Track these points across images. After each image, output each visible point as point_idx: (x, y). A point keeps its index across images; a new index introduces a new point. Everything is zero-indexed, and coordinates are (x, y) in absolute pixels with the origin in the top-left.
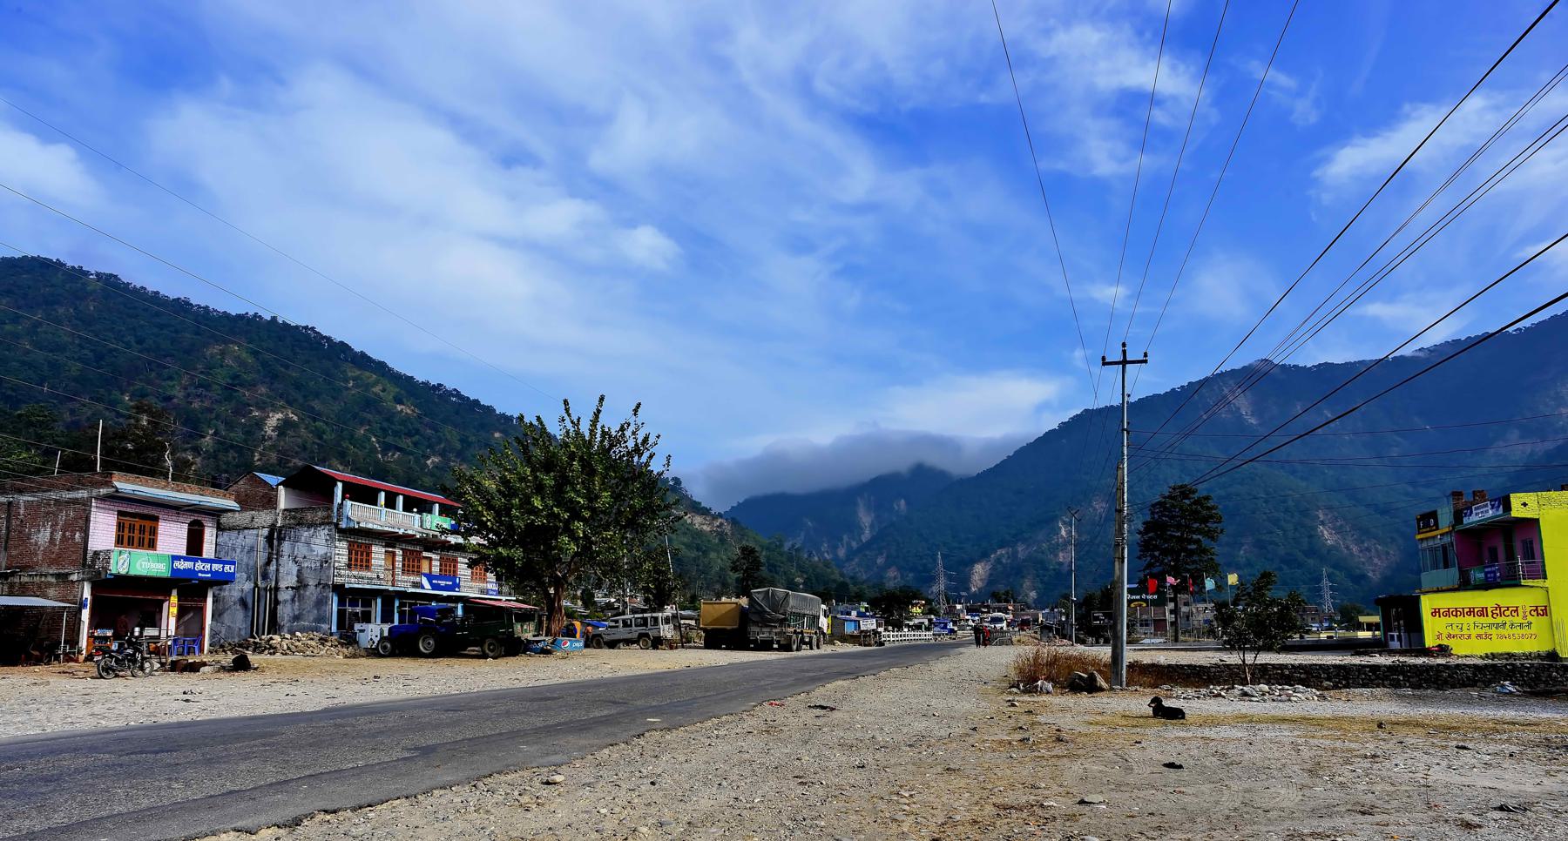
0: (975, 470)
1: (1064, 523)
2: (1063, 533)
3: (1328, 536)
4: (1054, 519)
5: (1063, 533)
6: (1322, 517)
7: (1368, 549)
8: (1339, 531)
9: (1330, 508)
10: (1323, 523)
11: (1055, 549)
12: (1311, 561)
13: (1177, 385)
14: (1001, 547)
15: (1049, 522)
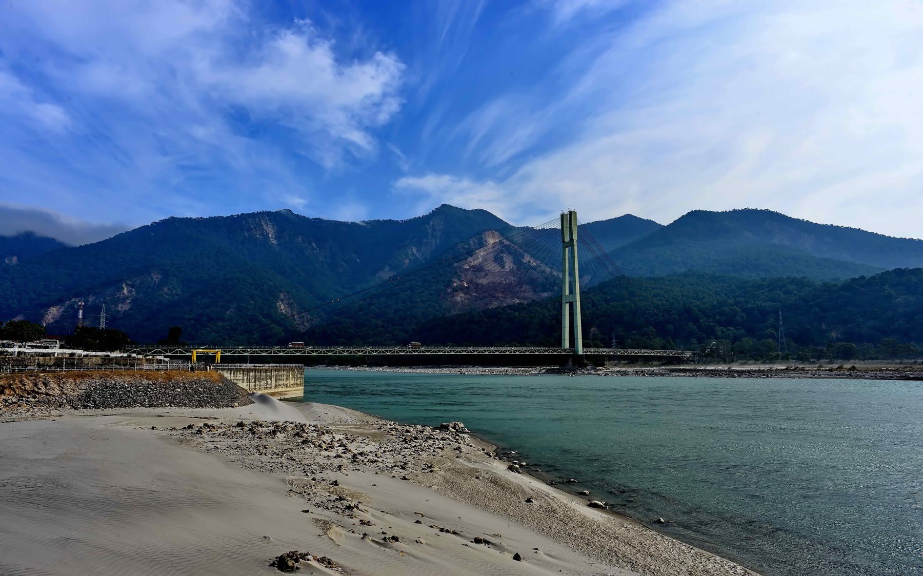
0: (77, 243)
1: (127, 285)
2: (125, 291)
3: (282, 307)
4: (121, 281)
5: (125, 291)
6: (282, 297)
7: (303, 317)
8: (290, 305)
9: (288, 293)
10: (282, 300)
11: (116, 301)
12: (265, 321)
13: (235, 214)
14: (76, 297)
15: (117, 283)
